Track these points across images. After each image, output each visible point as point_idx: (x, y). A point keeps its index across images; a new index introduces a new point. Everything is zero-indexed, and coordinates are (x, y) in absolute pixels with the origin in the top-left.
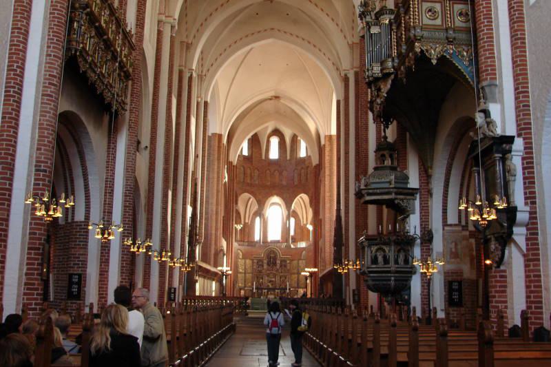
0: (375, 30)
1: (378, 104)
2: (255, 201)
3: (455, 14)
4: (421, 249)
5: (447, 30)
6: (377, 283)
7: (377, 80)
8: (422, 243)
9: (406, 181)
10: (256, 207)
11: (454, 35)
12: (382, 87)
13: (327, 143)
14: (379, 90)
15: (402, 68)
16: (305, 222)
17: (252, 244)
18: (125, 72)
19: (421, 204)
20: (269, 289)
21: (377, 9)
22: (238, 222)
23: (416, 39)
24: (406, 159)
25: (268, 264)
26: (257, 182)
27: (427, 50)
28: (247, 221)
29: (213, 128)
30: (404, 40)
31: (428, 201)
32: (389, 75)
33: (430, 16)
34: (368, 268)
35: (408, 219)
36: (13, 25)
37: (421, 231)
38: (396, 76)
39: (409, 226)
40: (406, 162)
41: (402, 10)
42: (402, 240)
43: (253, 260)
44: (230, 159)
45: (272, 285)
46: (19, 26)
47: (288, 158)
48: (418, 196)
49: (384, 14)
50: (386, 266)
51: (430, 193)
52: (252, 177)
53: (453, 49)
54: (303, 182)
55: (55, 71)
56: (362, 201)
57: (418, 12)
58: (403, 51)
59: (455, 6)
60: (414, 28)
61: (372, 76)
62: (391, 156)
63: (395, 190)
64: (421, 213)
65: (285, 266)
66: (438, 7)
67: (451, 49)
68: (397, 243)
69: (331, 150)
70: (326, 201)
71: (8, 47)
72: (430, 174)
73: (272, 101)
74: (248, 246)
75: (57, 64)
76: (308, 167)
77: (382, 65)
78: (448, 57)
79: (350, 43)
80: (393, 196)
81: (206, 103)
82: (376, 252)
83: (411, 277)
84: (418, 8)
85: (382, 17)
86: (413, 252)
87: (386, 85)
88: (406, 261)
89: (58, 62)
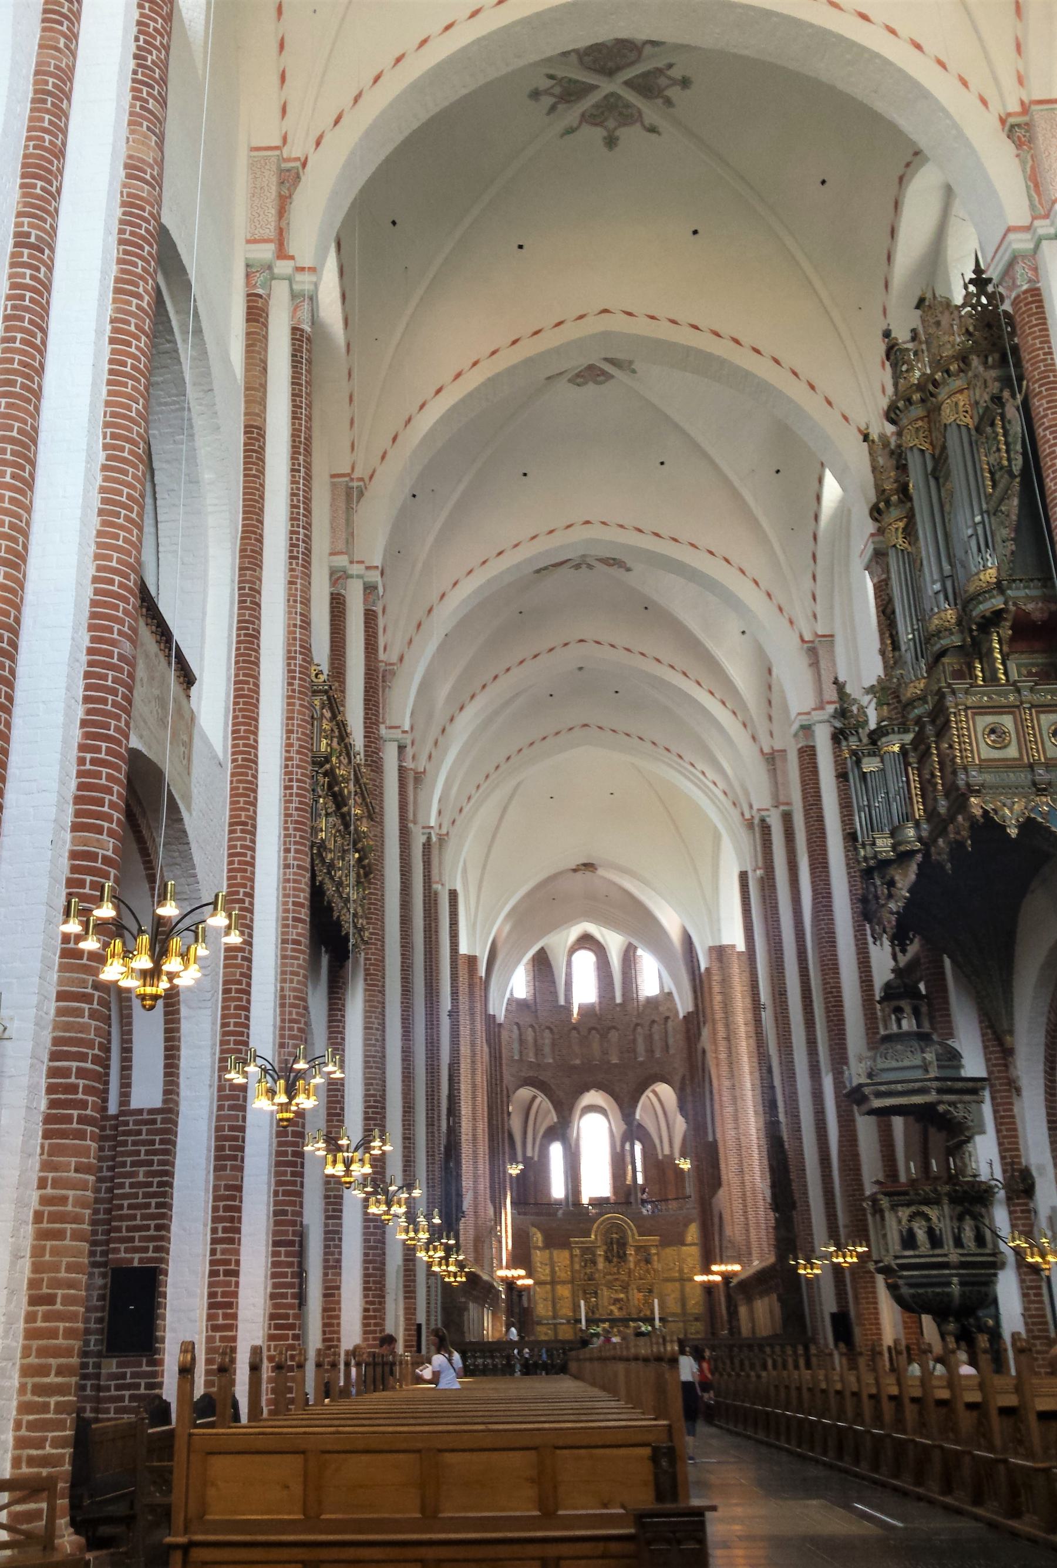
0: (870, 765)
1: (892, 913)
2: (547, 1104)
3: (1045, 733)
4: (1011, 1213)
5: (1031, 767)
6: (921, 1291)
7: (884, 865)
8: (1009, 1199)
9: (955, 1063)
10: (553, 1117)
11: (1047, 777)
12: (897, 878)
13: (715, 967)
14: (891, 884)
15: (941, 841)
16: (667, 1151)
17: (549, 1207)
18: (364, 867)
19: (995, 1112)
20: (613, 1322)
21: (872, 725)
22: (514, 1160)
23: (971, 790)
24: (949, 1015)
25: (608, 1260)
26: (551, 1061)
27: (996, 812)
28: (529, 1154)
29: (463, 949)
30: (940, 787)
31: (1011, 1104)
32: (911, 854)
33: (993, 741)
34: (896, 1257)
35: (970, 1147)
36: (231, 817)
37: (1004, 1171)
38: (927, 855)
39: (977, 1162)
40: (950, 1022)
41: (930, 729)
42: (965, 1192)
43: (571, 1249)
44: (491, 1013)
45: (621, 1309)
46: (243, 819)
47: (619, 1000)
48: (987, 1094)
49: (887, 734)
50: (938, 1251)
51: (1013, 1087)
52: (538, 1050)
53: (1048, 805)
54: (658, 1055)
55: (302, 895)
56: (865, 1108)
57: (969, 737)
58: (942, 810)
59: (1043, 717)
60: (965, 768)
61: (875, 857)
62: (916, 1013)
63: (935, 1084)
64: (998, 1131)
65: (648, 1261)
66: (1007, 722)
67: (1045, 804)
68: (954, 1200)
69: (726, 981)
70: (725, 1099)
71: (226, 860)
72: (1008, 1045)
73: (579, 875)
74: (537, 1214)
75: (303, 880)
76: (667, 1018)
77: (893, 834)
78: (1040, 820)
79: (767, 750)
80: (932, 1097)
81: (453, 895)
82: (909, 1221)
83: (995, 1275)
84: (968, 729)
85: (884, 740)
86: (992, 1219)
87: (906, 875)
88: (980, 1240)
89: (304, 877)
